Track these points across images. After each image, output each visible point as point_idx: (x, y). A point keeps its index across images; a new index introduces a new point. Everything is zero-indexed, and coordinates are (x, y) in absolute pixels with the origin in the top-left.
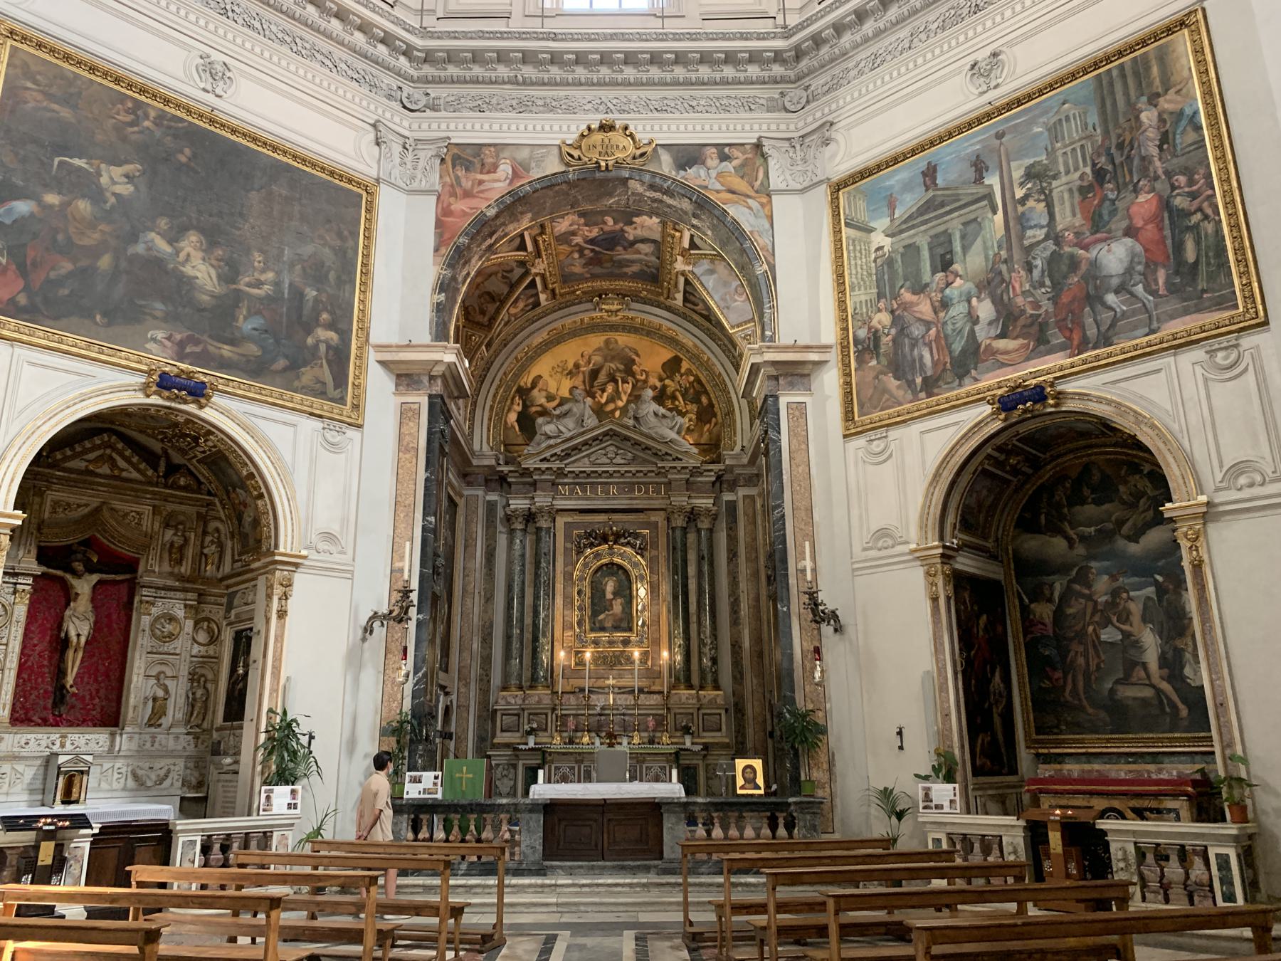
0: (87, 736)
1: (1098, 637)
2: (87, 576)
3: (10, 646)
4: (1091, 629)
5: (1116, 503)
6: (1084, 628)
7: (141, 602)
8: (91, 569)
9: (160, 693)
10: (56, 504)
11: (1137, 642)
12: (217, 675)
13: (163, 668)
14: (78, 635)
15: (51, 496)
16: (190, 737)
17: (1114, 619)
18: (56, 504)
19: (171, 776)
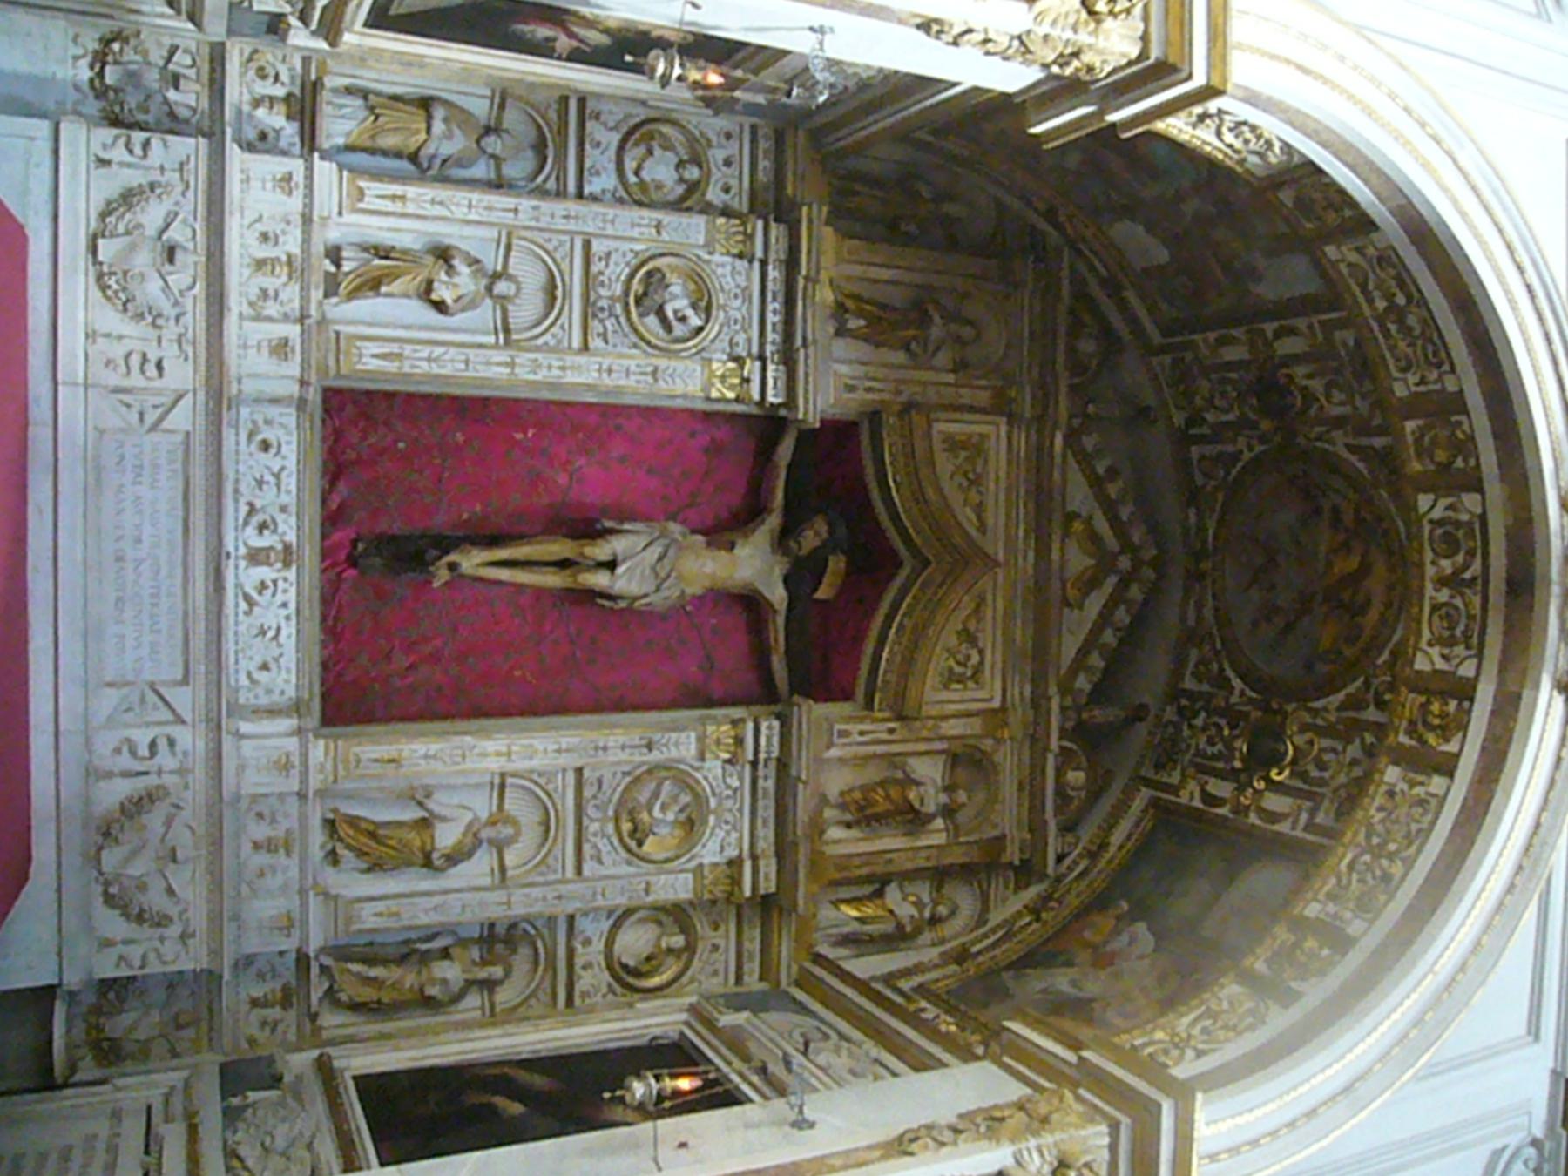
0: (290, 631)
2: (779, 569)
3: (582, 360)
7: (735, 723)
8: (801, 576)
9: (446, 837)
10: (974, 448)
12: (513, 1015)
13: (530, 836)
14: (611, 565)
15: (995, 431)
16: (289, 975)
18: (974, 448)
19: (146, 931)
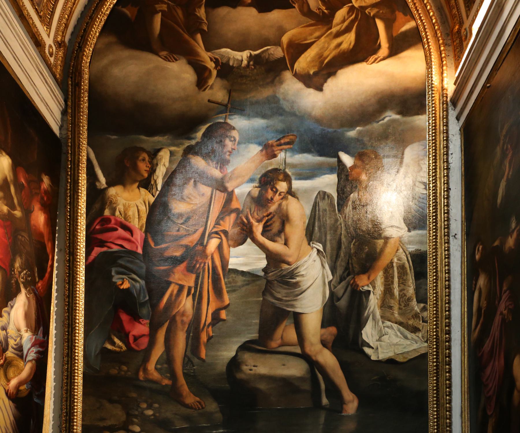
1: (224, 262)
4: (214, 243)
5: (295, 12)
6: (202, 242)
11: (292, 274)
17: (258, 229)
